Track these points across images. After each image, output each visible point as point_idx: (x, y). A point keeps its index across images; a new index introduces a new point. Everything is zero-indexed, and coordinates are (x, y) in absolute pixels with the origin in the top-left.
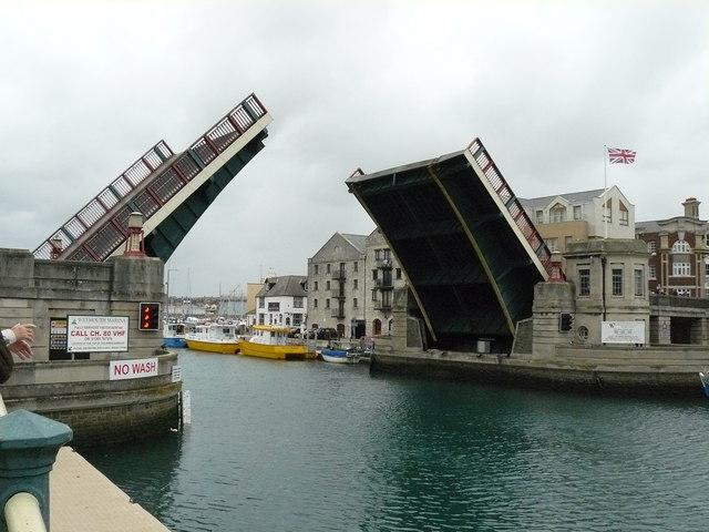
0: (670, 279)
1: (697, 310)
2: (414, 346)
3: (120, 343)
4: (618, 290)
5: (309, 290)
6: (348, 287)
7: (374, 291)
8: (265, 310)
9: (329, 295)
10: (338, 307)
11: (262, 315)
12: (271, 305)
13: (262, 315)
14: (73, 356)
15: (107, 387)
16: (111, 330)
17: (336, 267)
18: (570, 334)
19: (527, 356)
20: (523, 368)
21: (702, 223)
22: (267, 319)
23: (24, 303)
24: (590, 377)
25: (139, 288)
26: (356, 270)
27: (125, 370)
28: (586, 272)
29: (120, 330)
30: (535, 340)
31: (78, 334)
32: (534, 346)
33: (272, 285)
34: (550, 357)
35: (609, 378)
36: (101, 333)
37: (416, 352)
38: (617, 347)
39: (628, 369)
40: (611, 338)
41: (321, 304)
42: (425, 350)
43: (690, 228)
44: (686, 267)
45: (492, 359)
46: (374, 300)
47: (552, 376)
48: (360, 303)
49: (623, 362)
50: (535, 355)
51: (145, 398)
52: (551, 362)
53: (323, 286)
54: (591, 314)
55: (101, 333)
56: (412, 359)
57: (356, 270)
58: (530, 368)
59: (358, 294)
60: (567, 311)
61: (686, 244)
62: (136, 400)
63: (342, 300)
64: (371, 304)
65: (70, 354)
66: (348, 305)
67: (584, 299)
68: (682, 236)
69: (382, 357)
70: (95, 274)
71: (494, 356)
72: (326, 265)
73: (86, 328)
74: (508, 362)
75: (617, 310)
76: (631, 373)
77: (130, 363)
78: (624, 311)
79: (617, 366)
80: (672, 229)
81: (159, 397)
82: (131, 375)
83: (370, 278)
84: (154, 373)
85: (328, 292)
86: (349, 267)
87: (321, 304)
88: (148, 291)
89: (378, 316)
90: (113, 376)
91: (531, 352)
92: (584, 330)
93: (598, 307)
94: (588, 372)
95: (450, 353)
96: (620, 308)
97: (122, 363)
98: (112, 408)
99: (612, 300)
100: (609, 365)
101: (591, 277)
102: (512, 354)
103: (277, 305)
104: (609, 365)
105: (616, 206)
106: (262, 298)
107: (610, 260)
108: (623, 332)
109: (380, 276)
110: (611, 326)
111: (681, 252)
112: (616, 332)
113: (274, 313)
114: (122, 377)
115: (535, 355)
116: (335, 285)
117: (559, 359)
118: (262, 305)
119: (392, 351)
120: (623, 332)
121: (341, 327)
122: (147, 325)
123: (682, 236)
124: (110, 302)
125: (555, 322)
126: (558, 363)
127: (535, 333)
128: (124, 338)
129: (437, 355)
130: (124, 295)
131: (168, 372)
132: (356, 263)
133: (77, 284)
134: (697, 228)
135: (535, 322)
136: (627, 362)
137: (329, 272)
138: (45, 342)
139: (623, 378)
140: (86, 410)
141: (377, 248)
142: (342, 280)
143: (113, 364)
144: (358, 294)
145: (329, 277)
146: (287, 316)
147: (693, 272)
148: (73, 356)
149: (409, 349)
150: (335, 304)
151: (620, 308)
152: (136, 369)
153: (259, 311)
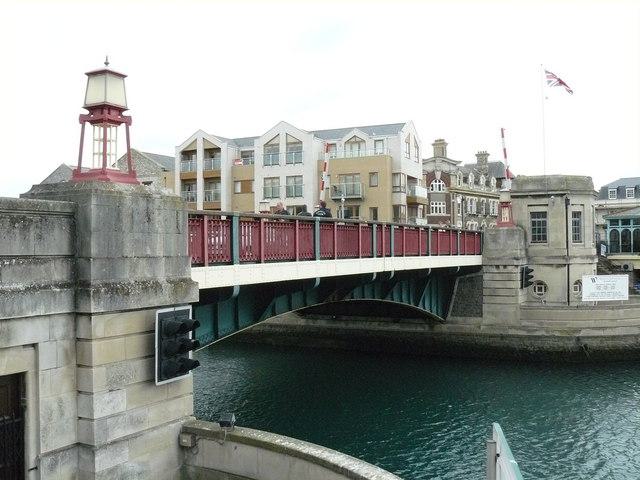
4: (577, 238)
19: (473, 320)
21: (454, 163)
24: (571, 344)
25: (144, 272)
28: (544, 214)
34: (512, 321)
35: (594, 344)
38: (601, 305)
39: (617, 332)
40: (593, 295)
43: (446, 168)
44: (442, 206)
47: (515, 344)
49: (609, 324)
54: (552, 265)
56: (277, 326)
58: (480, 335)
67: (539, 247)
68: (438, 175)
70: (32, 233)
75: (578, 261)
76: (619, 336)
78: (585, 261)
79: (604, 328)
88: (162, 278)
91: (480, 314)
93: (564, 257)
94: (569, 339)
96: (582, 257)
100: (594, 328)
101: (550, 221)
102: (449, 318)
104: (594, 328)
110: (593, 280)
111: (438, 191)
112: (598, 288)
117: (524, 323)
120: (606, 288)
123: (438, 175)
126: (524, 328)
127: (485, 292)
129: (322, 323)
134: (453, 168)
135: (486, 277)
136: (615, 324)
147: (448, 211)
151: (582, 257)
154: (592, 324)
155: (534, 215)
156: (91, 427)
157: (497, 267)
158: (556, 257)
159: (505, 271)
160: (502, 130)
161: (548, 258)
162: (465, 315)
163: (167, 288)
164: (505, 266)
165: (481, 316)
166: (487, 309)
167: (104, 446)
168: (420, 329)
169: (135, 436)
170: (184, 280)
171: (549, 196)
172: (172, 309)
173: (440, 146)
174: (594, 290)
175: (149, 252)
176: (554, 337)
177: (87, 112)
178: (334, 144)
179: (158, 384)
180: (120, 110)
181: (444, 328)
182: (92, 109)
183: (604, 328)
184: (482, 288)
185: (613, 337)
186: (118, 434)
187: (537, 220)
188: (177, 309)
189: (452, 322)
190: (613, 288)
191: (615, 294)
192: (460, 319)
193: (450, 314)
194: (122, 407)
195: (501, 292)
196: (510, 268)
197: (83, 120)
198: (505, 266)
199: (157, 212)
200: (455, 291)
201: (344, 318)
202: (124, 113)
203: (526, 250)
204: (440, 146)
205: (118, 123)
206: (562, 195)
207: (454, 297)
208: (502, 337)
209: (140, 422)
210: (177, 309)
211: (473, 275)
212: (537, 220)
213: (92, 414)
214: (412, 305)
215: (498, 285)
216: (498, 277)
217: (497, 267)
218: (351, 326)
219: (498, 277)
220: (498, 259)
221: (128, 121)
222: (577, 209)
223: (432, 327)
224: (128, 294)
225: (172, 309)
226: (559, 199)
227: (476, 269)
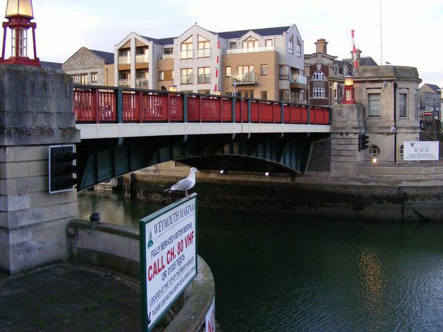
0: (311, 100)
4: (404, 114)
19: (324, 174)
21: (333, 58)
24: (395, 192)
25: (41, 122)
30: (333, 158)
32: (332, 165)
34: (352, 174)
38: (415, 163)
40: (412, 156)
43: (326, 62)
44: (322, 91)
47: (354, 192)
49: (424, 178)
52: (353, 179)
54: (383, 133)
60: (363, 131)
61: (322, 74)
68: (319, 67)
75: (404, 130)
76: (430, 187)
79: (418, 181)
88: (54, 126)
91: (329, 170)
94: (393, 188)
96: (406, 128)
100: (410, 181)
102: (306, 172)
104: (410, 181)
105: (295, 40)
107: (400, 85)
108: (422, 151)
110: (412, 145)
111: (322, 79)
112: (416, 150)
123: (319, 67)
125: (357, 142)
126: (360, 180)
127: (333, 153)
135: (333, 142)
136: (427, 178)
147: (327, 96)
151: (406, 128)
154: (410, 177)
156: (6, 216)
157: (341, 134)
160: (353, 31)
163: (58, 134)
164: (347, 134)
165: (330, 171)
166: (334, 166)
167: (15, 229)
168: (284, 181)
169: (37, 225)
170: (71, 128)
171: (382, 81)
172: (60, 146)
173: (322, 43)
174: (414, 152)
175: (45, 109)
176: (381, 186)
177: (7, 20)
178: (235, 43)
179: (50, 192)
180: (29, 18)
181: (300, 180)
182: (10, 18)
184: (330, 150)
186: (25, 222)
188: (64, 146)
189: (308, 176)
190: (427, 150)
191: (429, 155)
193: (306, 169)
194: (27, 206)
195: (344, 153)
196: (350, 135)
197: (5, 25)
198: (347, 134)
199: (51, 84)
200: (311, 152)
201: (230, 172)
202: (32, 21)
203: (365, 122)
204: (322, 43)
205: (28, 27)
206: (391, 81)
207: (310, 156)
208: (344, 187)
209: (39, 216)
210: (64, 146)
211: (324, 140)
213: (7, 209)
214: (274, 161)
215: (342, 148)
216: (342, 142)
217: (341, 134)
218: (235, 178)
219: (342, 142)
220: (342, 128)
221: (34, 26)
222: (404, 91)
223: (293, 179)
224: (30, 135)
225: (60, 146)
226: (389, 83)
227: (326, 135)
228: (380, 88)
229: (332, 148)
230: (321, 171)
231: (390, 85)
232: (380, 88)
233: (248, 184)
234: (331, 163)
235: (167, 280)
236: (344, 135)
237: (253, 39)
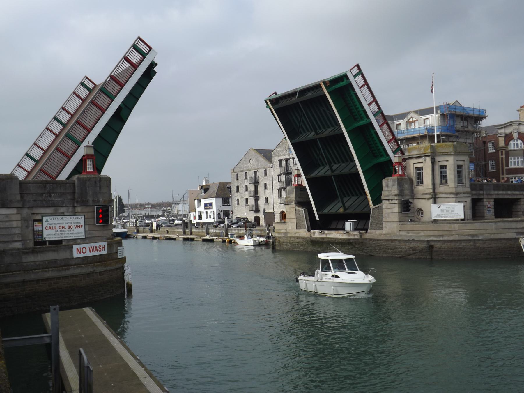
0: (506, 169)
1: (517, 193)
2: (301, 228)
3: (80, 233)
5: (233, 192)
6: (261, 188)
7: (280, 190)
8: (202, 209)
9: (247, 195)
10: (254, 203)
11: (200, 213)
12: (206, 205)
13: (200, 213)
14: (48, 243)
15: (73, 262)
16: (73, 225)
17: (251, 174)
18: (410, 214)
19: (378, 232)
20: (378, 240)
22: (204, 216)
23: (14, 211)
26: (265, 175)
27: (84, 251)
28: (421, 168)
29: (79, 225)
30: (384, 219)
31: (50, 228)
32: (384, 224)
33: (206, 190)
36: (66, 226)
37: (304, 233)
40: (439, 215)
41: (243, 202)
42: (309, 231)
44: (520, 160)
45: (356, 235)
46: (280, 196)
48: (270, 200)
50: (385, 231)
51: (100, 269)
53: (242, 189)
55: (66, 226)
57: (265, 175)
58: (381, 240)
59: (268, 193)
61: (520, 142)
62: (92, 270)
63: (257, 199)
64: (277, 200)
65: (46, 242)
66: (261, 202)
68: (515, 135)
69: (280, 237)
71: (356, 233)
72: (243, 173)
73: (55, 224)
74: (367, 236)
77: (87, 246)
78: (449, 196)
79: (442, 236)
80: (508, 131)
81: (109, 268)
82: (88, 254)
83: (276, 182)
84: (105, 252)
85: (247, 193)
86: (260, 174)
87: (243, 202)
89: (283, 208)
90: (76, 255)
91: (381, 228)
92: (420, 211)
95: (326, 232)
96: (446, 193)
97: (82, 246)
98: (77, 276)
99: (441, 189)
101: (424, 172)
102: (369, 231)
103: (211, 205)
106: (200, 200)
107: (438, 159)
108: (447, 211)
109: (283, 178)
112: (442, 211)
113: (209, 211)
114: (82, 255)
115: (385, 231)
116: (251, 188)
118: (200, 205)
119: (286, 233)
121: (257, 219)
122: (101, 221)
123: (515, 135)
124: (74, 207)
125: (397, 206)
127: (384, 215)
128: (82, 230)
130: (84, 203)
131: (115, 251)
132: (265, 171)
133: (50, 196)
135: (384, 206)
137: (246, 178)
138: (31, 237)
139: (457, 245)
140: (59, 278)
141: (281, 158)
142: (256, 183)
143: (75, 247)
144: (268, 193)
145: (246, 182)
146: (219, 212)
148: (48, 243)
149: (298, 231)
150: (252, 202)
151: (446, 193)
152: (91, 249)
153: (198, 209)
155: (418, 169)
157: (388, 200)
158: (426, 194)
159: (392, 202)
161: (423, 194)
162: (376, 229)
164: (392, 200)
171: (422, 157)
174: (440, 213)
183: (442, 236)
185: (451, 241)
187: (419, 172)
189: (371, 233)
190: (452, 211)
191: (454, 215)
192: (373, 231)
193: (369, 229)
195: (391, 215)
198: (392, 200)
206: (428, 156)
212: (419, 172)
217: (388, 200)
219: (389, 206)
228: (422, 163)
229: (383, 212)
230: (378, 229)
231: (428, 159)
232: (422, 163)
233: (337, 240)
234: (383, 223)
235: (57, 233)
236: (390, 201)
237: (414, 119)
